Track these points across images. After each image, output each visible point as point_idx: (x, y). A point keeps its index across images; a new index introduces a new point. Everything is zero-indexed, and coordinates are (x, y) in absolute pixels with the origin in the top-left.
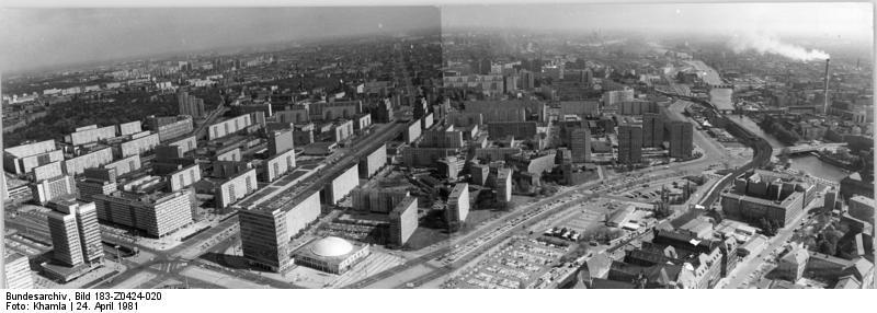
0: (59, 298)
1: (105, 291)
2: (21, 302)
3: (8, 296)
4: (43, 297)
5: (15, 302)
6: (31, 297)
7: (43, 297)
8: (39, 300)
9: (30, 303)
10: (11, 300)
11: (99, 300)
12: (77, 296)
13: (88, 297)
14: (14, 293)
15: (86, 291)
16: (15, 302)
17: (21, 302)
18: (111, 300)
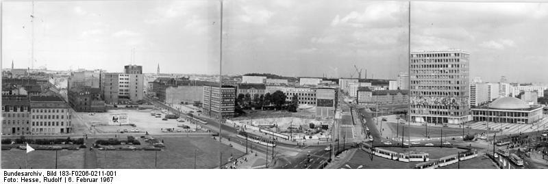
0: (37, 175)
1: (66, 170)
2: (13, 177)
3: (5, 173)
4: (27, 174)
5: (10, 177)
6: (19, 174)
7: (27, 174)
10: (7, 176)
12: (48, 173)
15: (54, 170)
16: (10, 177)
17: (13, 177)
18: (70, 176)
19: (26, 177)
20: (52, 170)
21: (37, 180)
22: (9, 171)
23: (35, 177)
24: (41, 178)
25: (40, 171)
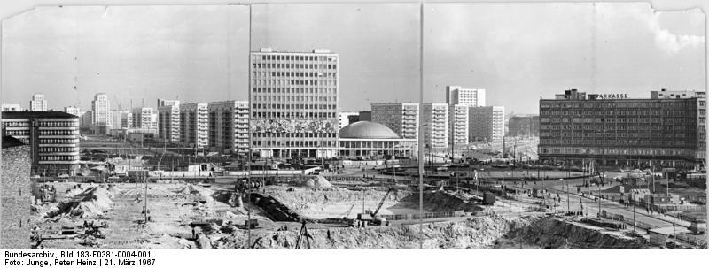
0: (48, 256)
2: (17, 259)
3: (7, 254)
4: (35, 255)
5: (12, 259)
6: (25, 255)
7: (35, 255)
8: (31, 258)
9: (25, 260)
10: (9, 258)
11: (80, 258)
12: (63, 254)
13: (71, 255)
14: (12, 251)
16: (12, 259)
17: (17, 259)
19: (35, 259)
20: (67, 250)
21: (46, 263)
22: (12, 251)
23: (44, 259)
24: (51, 261)
25: (51, 251)
